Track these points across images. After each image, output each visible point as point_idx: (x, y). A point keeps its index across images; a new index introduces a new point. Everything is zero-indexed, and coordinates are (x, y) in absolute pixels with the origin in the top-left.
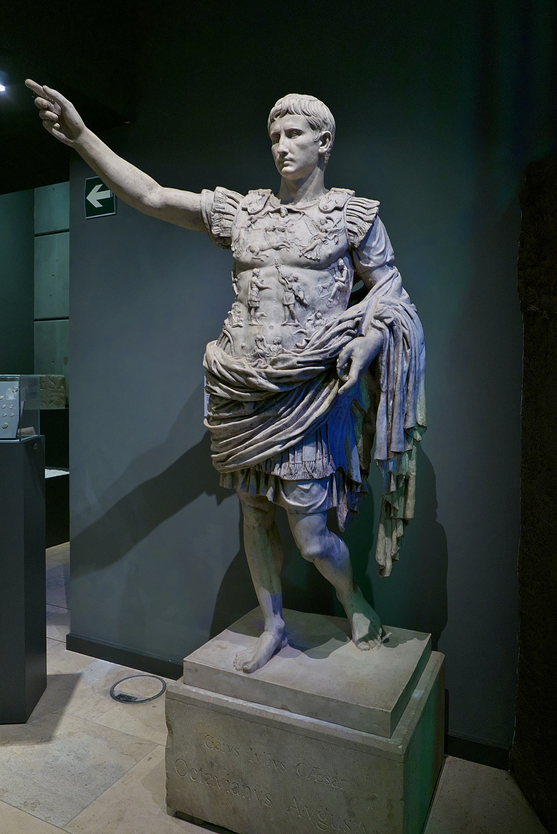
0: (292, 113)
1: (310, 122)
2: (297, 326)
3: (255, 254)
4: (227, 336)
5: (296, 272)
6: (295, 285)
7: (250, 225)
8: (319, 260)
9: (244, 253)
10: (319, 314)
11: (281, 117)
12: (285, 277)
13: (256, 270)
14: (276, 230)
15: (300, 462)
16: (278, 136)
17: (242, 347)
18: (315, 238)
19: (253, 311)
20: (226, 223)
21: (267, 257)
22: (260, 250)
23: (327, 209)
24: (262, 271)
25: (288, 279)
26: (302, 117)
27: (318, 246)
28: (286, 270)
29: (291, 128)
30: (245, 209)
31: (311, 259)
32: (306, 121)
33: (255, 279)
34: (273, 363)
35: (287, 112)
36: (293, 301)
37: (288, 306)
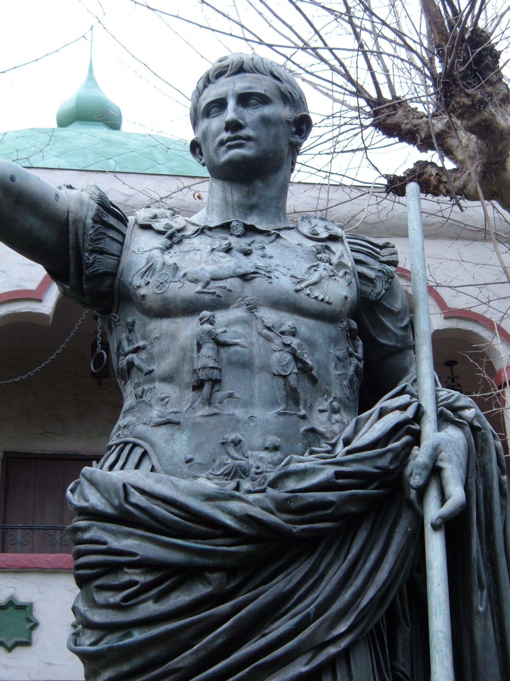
12: (272, 326)
14: (234, 252)
26: (269, 78)
34: (273, 484)
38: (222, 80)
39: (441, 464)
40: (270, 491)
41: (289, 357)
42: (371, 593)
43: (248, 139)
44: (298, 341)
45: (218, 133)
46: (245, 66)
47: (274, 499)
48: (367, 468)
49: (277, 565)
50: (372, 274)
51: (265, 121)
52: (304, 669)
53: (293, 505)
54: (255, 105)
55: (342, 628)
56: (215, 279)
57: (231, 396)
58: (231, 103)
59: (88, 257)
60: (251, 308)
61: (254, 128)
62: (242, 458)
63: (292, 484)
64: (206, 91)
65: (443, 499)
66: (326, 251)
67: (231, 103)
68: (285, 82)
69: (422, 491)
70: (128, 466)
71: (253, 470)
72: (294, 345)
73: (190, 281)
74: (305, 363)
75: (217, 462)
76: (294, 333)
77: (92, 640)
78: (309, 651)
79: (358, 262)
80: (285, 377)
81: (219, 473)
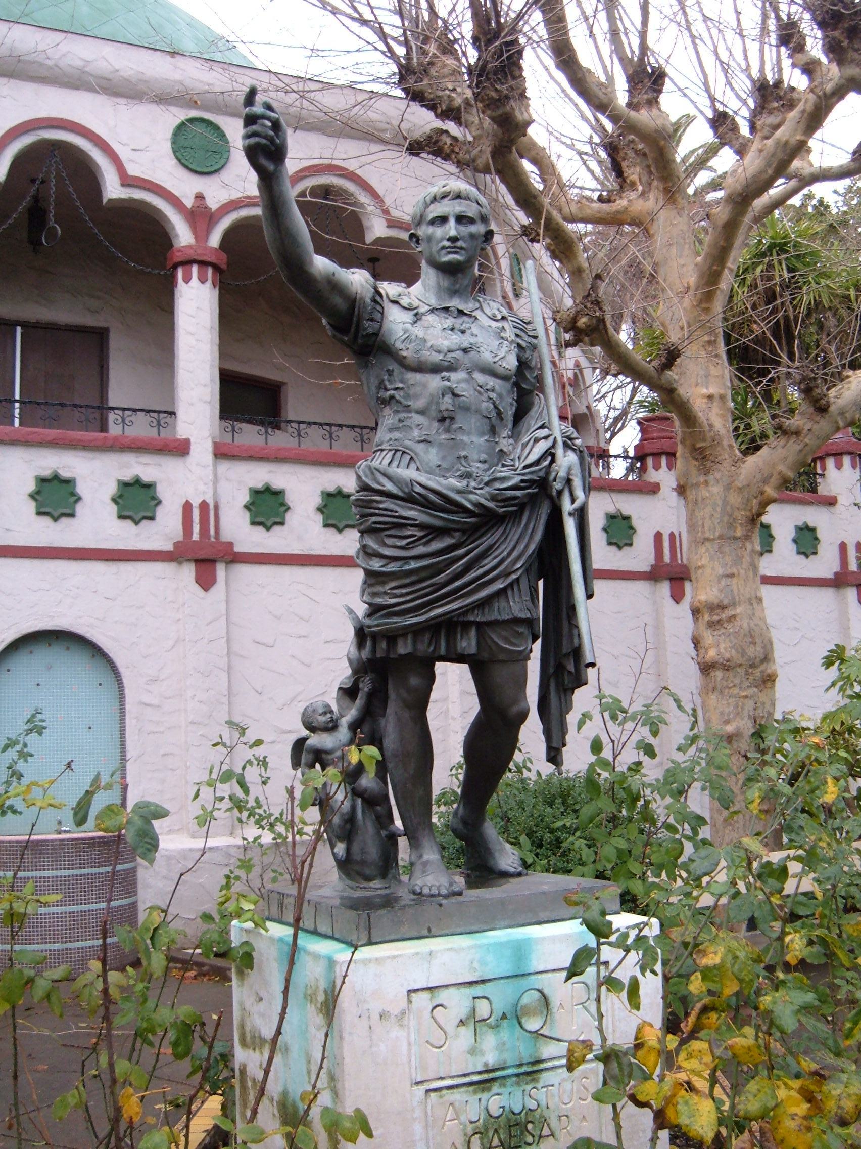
4: (404, 452)
5: (491, 382)
13: (444, 374)
14: (456, 331)
24: (454, 376)
26: (475, 205)
28: (480, 378)
33: (447, 383)
36: (494, 414)
38: (445, 201)
39: (571, 477)
41: (492, 406)
43: (462, 248)
45: (442, 240)
48: (534, 477)
49: (485, 529)
50: (524, 344)
52: (501, 586)
53: (500, 498)
55: (519, 566)
56: (450, 351)
57: (461, 428)
59: (366, 324)
65: (573, 501)
67: (452, 222)
69: (560, 493)
70: (402, 464)
74: (499, 410)
77: (381, 564)
80: (489, 418)
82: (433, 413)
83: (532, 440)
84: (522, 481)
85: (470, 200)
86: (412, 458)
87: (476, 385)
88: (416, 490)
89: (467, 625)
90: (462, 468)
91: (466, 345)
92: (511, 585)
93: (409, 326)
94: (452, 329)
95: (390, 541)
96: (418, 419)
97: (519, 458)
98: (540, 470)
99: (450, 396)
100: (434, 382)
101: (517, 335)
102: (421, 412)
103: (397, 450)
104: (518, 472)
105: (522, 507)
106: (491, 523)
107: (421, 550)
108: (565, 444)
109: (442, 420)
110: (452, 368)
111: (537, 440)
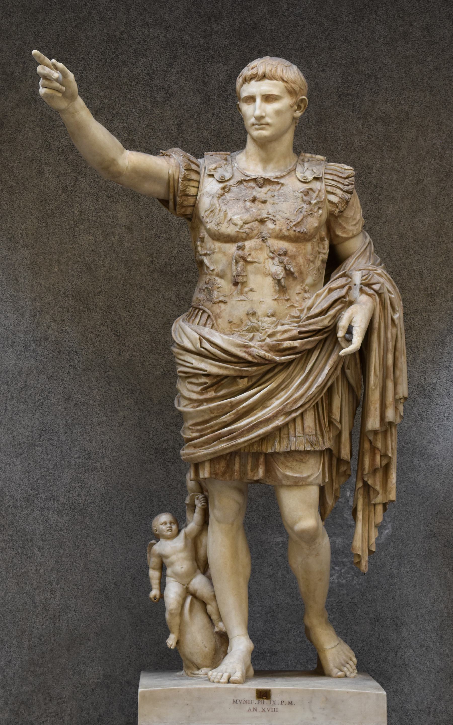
0: (270, 79)
1: (288, 88)
2: (287, 300)
3: (239, 227)
4: (204, 311)
6: (286, 259)
7: (223, 195)
8: (306, 233)
9: (225, 225)
10: (307, 288)
11: (257, 81)
12: (274, 251)
13: (240, 244)
14: (257, 202)
15: (301, 435)
16: (252, 99)
17: (230, 322)
18: (300, 211)
19: (239, 286)
20: (192, 191)
21: (253, 230)
22: (244, 223)
23: (306, 179)
24: (248, 244)
25: (276, 253)
26: (281, 83)
27: (304, 219)
29: (270, 93)
30: (212, 176)
31: (299, 232)
32: (283, 87)
33: (240, 252)
35: (264, 77)
37: (279, 281)
38: (253, 82)
40: (268, 340)
42: (313, 389)
43: (268, 124)
44: (287, 258)
46: (267, 76)
47: (268, 346)
51: (278, 113)
54: (272, 101)
56: (245, 223)
58: (258, 100)
60: (264, 240)
61: (271, 118)
62: (256, 321)
63: (279, 337)
64: (245, 86)
66: (310, 192)
68: (290, 83)
71: (261, 328)
72: (285, 261)
73: (233, 224)
74: (289, 270)
75: (244, 323)
76: (285, 254)
77: (185, 404)
78: (282, 415)
79: (329, 192)
81: (245, 329)
82: (229, 276)
83: (327, 291)
84: (300, 333)
85: (276, 79)
86: (209, 316)
87: (268, 251)
88: (204, 346)
89: (256, 456)
90: (250, 323)
91: (264, 215)
92: (294, 420)
93: (215, 201)
94: (254, 200)
95: (189, 386)
96: (219, 280)
97: (309, 309)
98: (326, 318)
99: (241, 263)
100: (232, 249)
101: (329, 192)
102: (222, 277)
103: (200, 309)
104: (301, 323)
105: (310, 352)
106: (276, 370)
107: (211, 394)
108: (361, 290)
109: (236, 284)
110: (248, 237)
111: (331, 290)
